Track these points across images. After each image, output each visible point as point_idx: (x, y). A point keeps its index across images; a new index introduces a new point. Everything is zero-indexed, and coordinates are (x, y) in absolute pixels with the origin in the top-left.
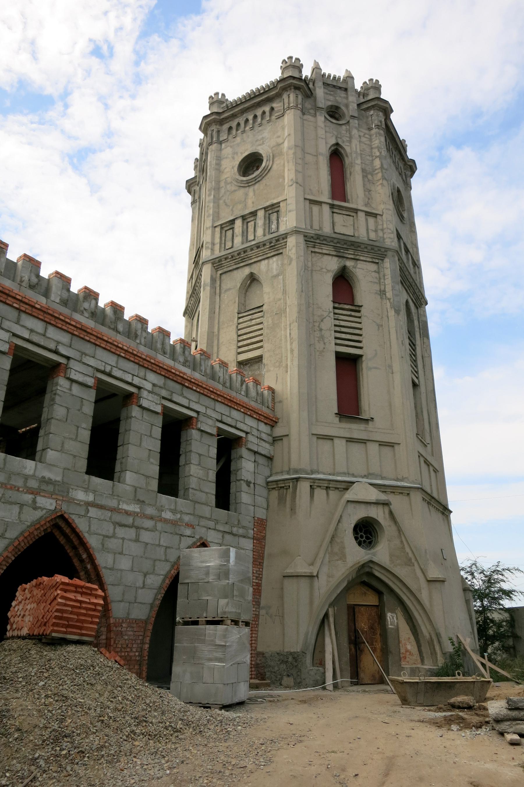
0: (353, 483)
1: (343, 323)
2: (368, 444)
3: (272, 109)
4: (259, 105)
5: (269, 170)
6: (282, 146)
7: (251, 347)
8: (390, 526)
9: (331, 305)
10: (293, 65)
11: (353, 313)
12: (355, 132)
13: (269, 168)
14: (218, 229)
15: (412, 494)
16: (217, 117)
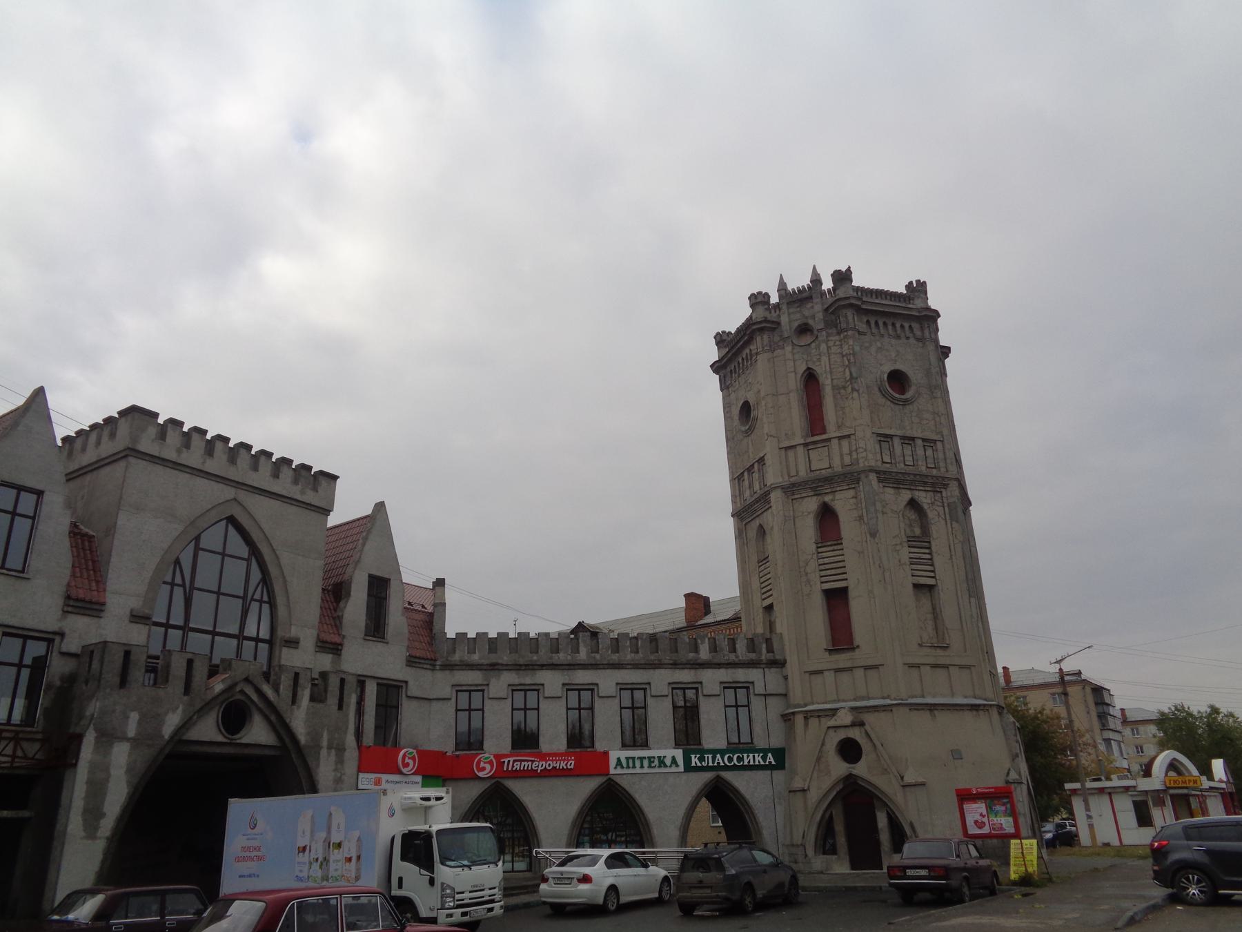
1: (826, 560)
4: (743, 347)
10: (758, 300)
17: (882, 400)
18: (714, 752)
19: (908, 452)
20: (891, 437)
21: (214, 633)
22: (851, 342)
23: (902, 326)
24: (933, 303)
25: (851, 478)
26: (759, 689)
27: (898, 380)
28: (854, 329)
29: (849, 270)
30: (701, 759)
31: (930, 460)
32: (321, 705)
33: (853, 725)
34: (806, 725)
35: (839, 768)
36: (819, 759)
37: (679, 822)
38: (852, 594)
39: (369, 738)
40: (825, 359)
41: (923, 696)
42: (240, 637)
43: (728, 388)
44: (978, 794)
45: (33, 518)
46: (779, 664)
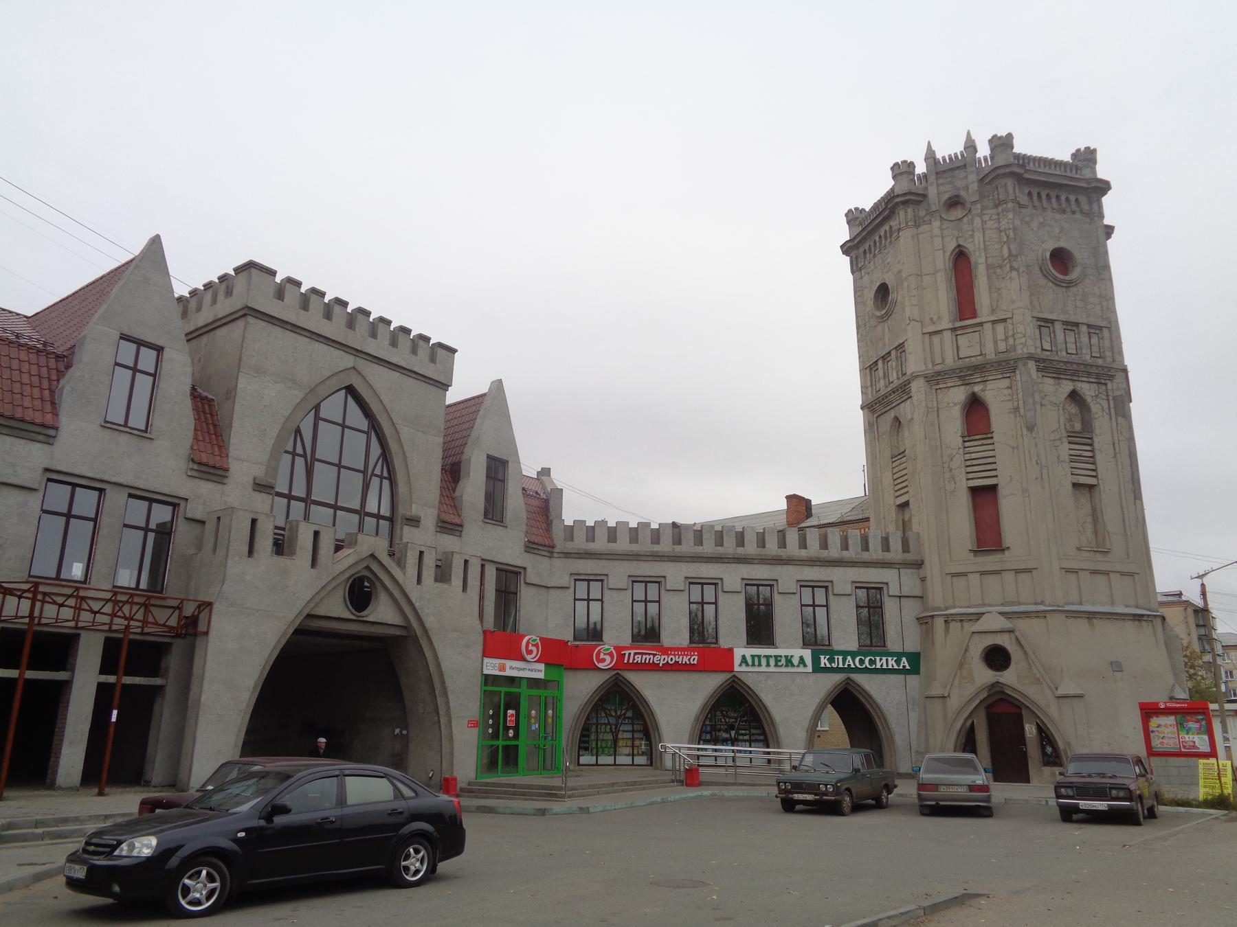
1: (974, 456)
4: (881, 224)
9: (960, 440)
10: (902, 170)
11: (984, 442)
17: (1043, 281)
18: (845, 654)
19: (1070, 338)
20: (1052, 321)
21: (336, 507)
22: (1010, 215)
23: (1067, 199)
24: (1102, 172)
25: (1006, 366)
26: (894, 590)
27: (1061, 258)
28: (1015, 201)
29: (1010, 136)
30: (831, 660)
31: (1095, 349)
32: (445, 586)
34: (947, 630)
35: (984, 676)
36: (961, 666)
37: (806, 724)
38: (1002, 492)
39: (490, 623)
40: (978, 235)
41: (1081, 604)
42: (362, 513)
43: (860, 269)
44: (1166, 708)
45: (154, 375)
46: (919, 565)
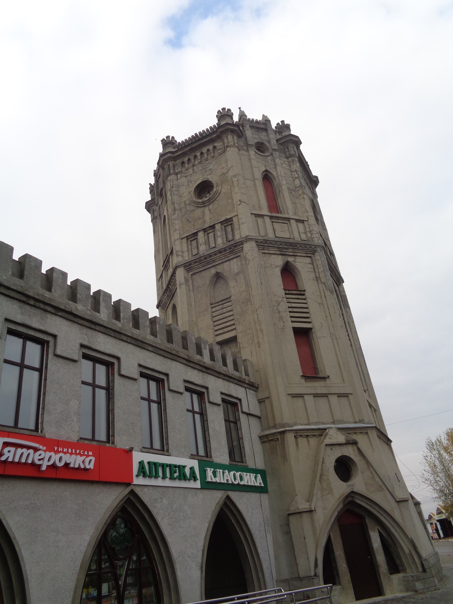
0: (325, 429)
1: (294, 305)
2: (330, 396)
3: (215, 147)
4: (204, 144)
5: (220, 193)
6: (227, 175)
7: (226, 330)
8: (360, 460)
9: (283, 292)
11: (300, 297)
12: (277, 161)
13: (219, 192)
14: (185, 240)
15: (369, 432)
16: (172, 155)
33: (348, 443)
34: (297, 444)
